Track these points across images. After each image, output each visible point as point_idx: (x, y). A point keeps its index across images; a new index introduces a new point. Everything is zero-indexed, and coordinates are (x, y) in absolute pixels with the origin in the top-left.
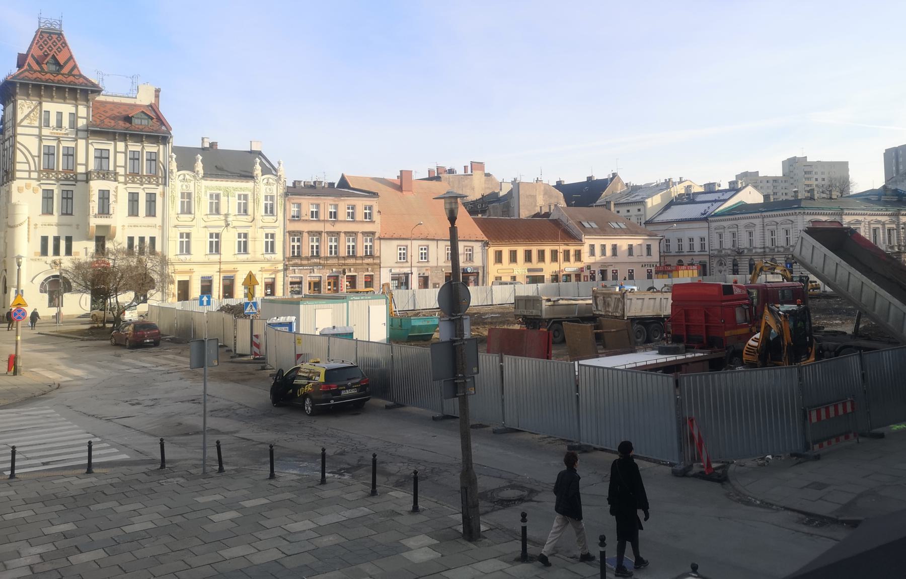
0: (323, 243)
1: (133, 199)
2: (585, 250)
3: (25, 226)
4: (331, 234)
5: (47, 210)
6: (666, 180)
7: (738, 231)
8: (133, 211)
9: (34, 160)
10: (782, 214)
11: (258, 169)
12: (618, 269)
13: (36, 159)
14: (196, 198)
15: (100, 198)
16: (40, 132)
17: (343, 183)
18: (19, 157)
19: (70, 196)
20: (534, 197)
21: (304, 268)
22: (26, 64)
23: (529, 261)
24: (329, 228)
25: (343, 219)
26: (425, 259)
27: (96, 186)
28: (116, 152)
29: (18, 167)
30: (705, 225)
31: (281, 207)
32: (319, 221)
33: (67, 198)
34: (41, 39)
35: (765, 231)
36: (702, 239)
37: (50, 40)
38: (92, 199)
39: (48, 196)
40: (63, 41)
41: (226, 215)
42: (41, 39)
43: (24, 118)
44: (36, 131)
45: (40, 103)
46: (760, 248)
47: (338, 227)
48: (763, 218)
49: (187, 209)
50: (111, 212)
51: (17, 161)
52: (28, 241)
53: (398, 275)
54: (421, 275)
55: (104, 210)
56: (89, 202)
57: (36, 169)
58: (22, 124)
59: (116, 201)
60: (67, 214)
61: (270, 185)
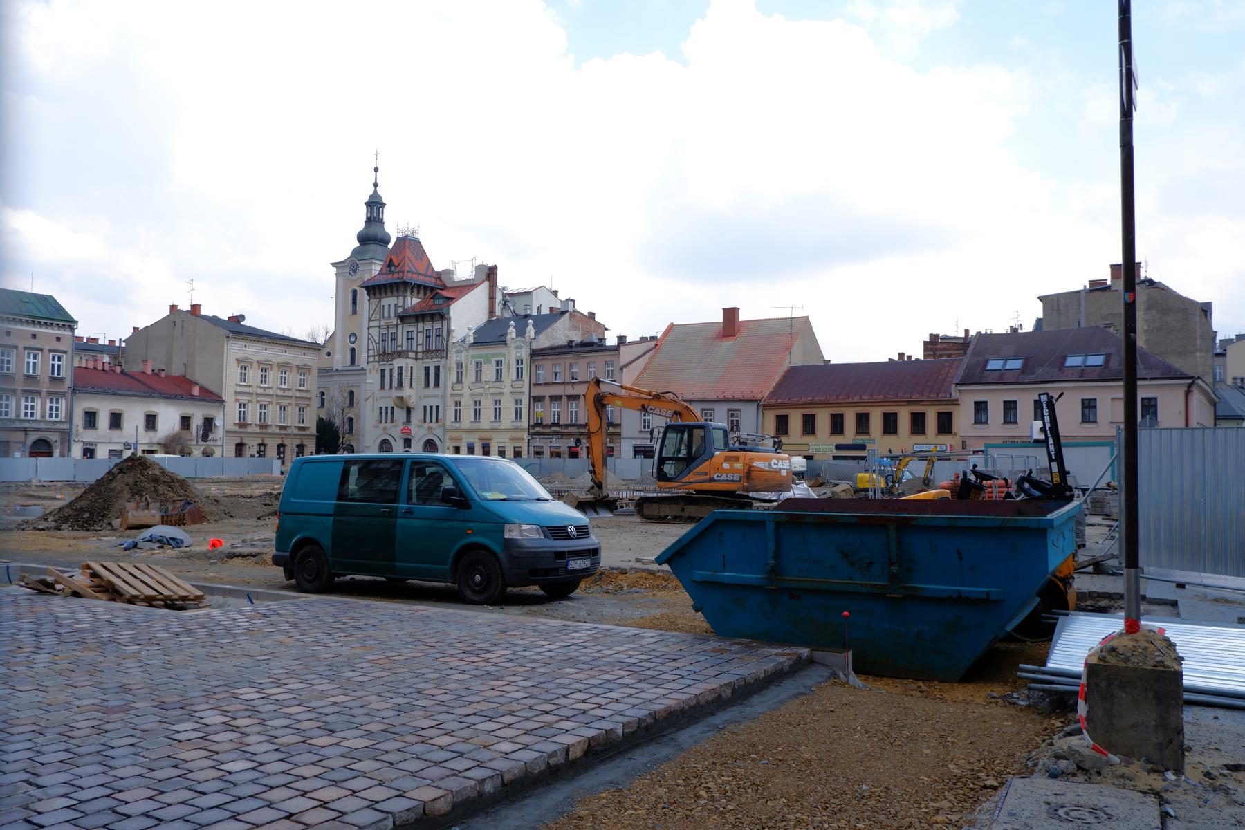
21: (546, 437)
24: (569, 391)
28: (418, 332)
45: (380, 300)
53: (643, 449)
58: (373, 318)
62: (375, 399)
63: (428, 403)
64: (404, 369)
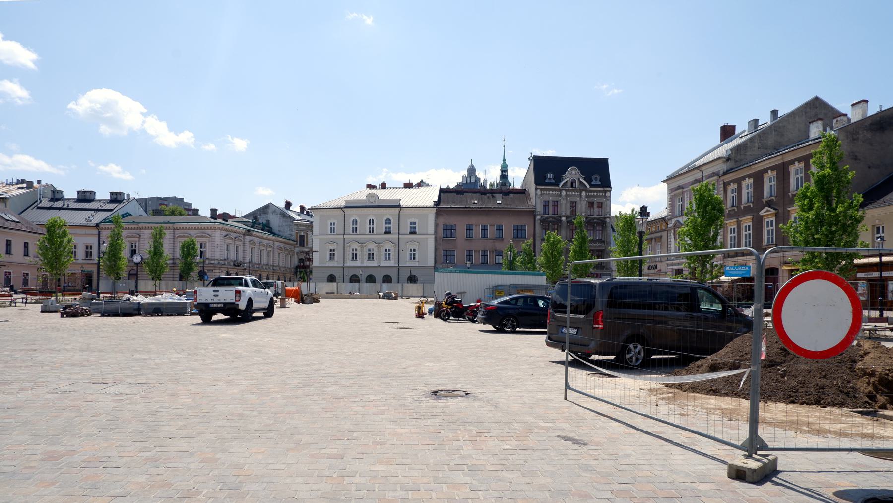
6: (18, 180)
7: (139, 241)
10: (189, 228)
12: (11, 271)
35: (176, 243)
36: (88, 247)
46: (170, 260)
48: (174, 230)
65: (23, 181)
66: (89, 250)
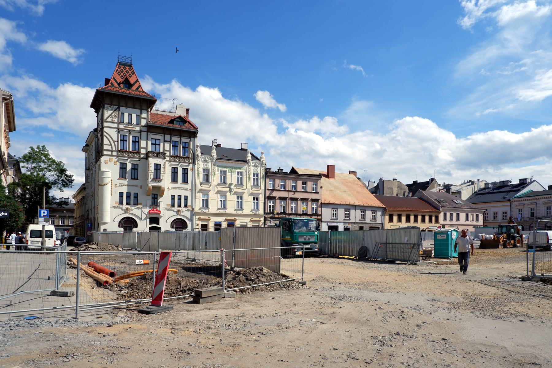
0: (287, 205)
1: (175, 172)
2: (441, 216)
3: (109, 185)
4: (293, 199)
5: (123, 176)
8: (174, 179)
9: (114, 143)
11: (249, 157)
13: (116, 143)
14: (212, 173)
15: (154, 169)
16: (118, 126)
17: (293, 171)
18: (106, 141)
19: (136, 168)
20: (392, 189)
22: (110, 83)
23: (408, 221)
24: (291, 195)
25: (300, 190)
26: (348, 217)
27: (152, 161)
29: (105, 147)
30: (508, 204)
31: (263, 181)
32: (286, 191)
33: (135, 169)
34: (119, 68)
37: (125, 69)
38: (150, 169)
39: (123, 167)
40: (132, 70)
41: (231, 185)
42: (119, 68)
43: (109, 117)
44: (115, 125)
47: (297, 195)
49: (207, 179)
50: (161, 178)
51: (104, 143)
52: (111, 195)
54: (346, 227)
55: (158, 177)
56: (148, 171)
57: (115, 149)
58: (108, 120)
59: (164, 171)
60: (135, 179)
61: (256, 167)
62: (113, 186)
63: (176, 193)
64: (162, 166)
65: (470, 181)
66: (496, 215)
